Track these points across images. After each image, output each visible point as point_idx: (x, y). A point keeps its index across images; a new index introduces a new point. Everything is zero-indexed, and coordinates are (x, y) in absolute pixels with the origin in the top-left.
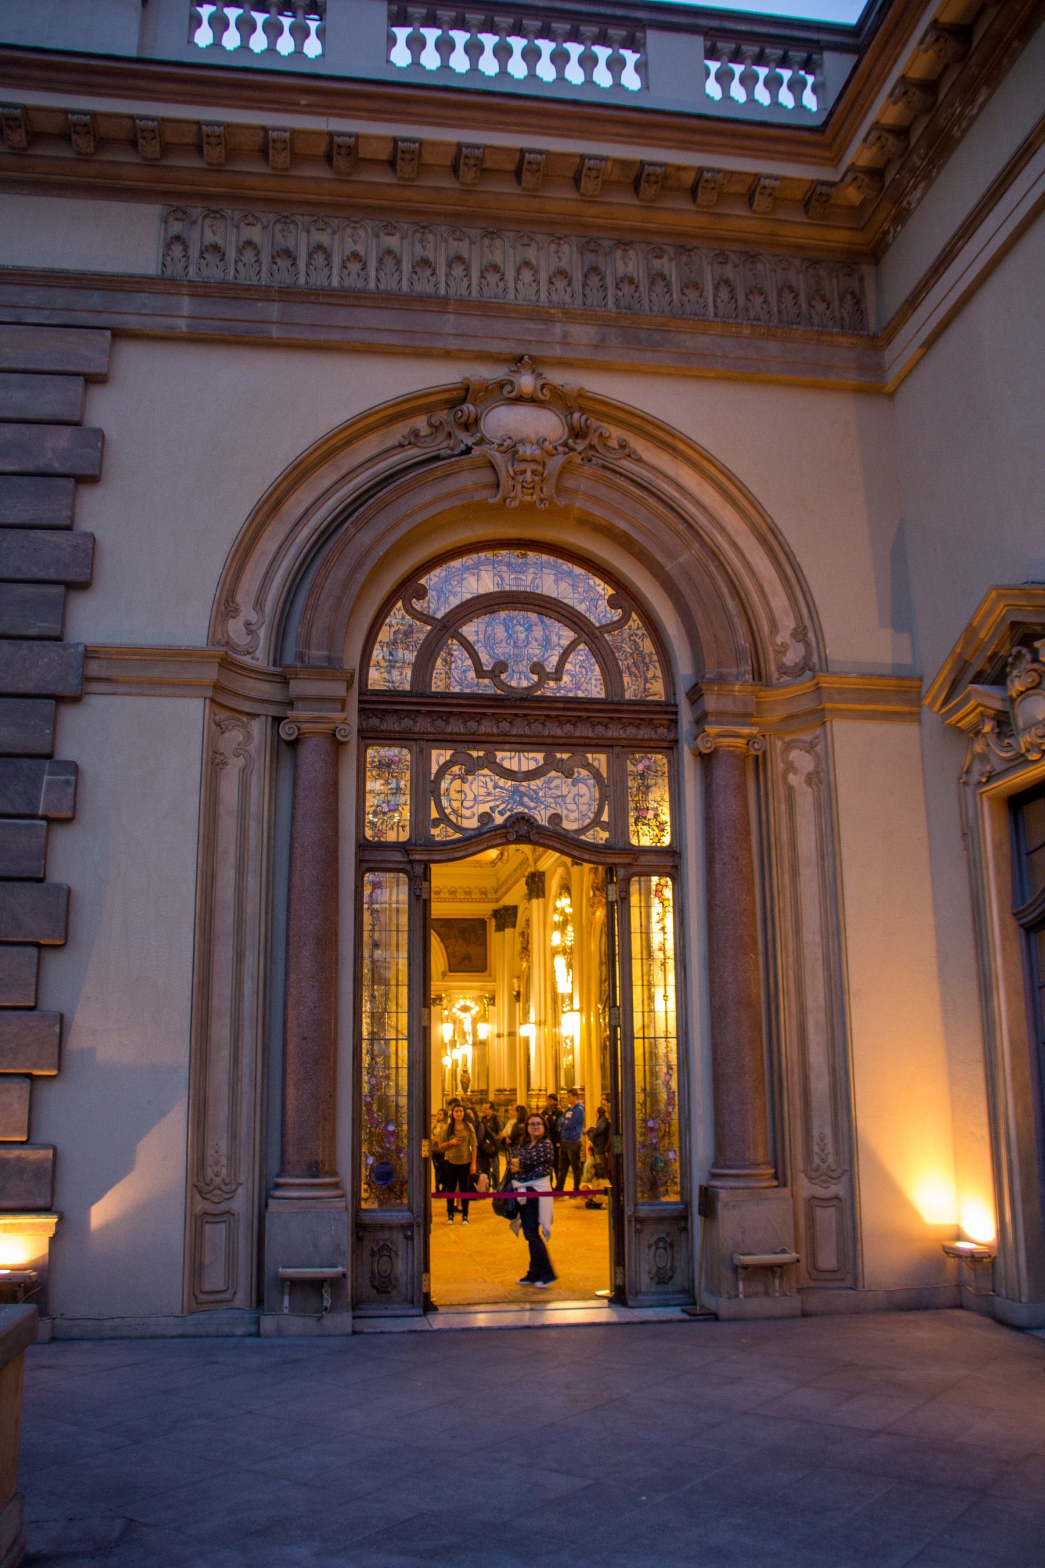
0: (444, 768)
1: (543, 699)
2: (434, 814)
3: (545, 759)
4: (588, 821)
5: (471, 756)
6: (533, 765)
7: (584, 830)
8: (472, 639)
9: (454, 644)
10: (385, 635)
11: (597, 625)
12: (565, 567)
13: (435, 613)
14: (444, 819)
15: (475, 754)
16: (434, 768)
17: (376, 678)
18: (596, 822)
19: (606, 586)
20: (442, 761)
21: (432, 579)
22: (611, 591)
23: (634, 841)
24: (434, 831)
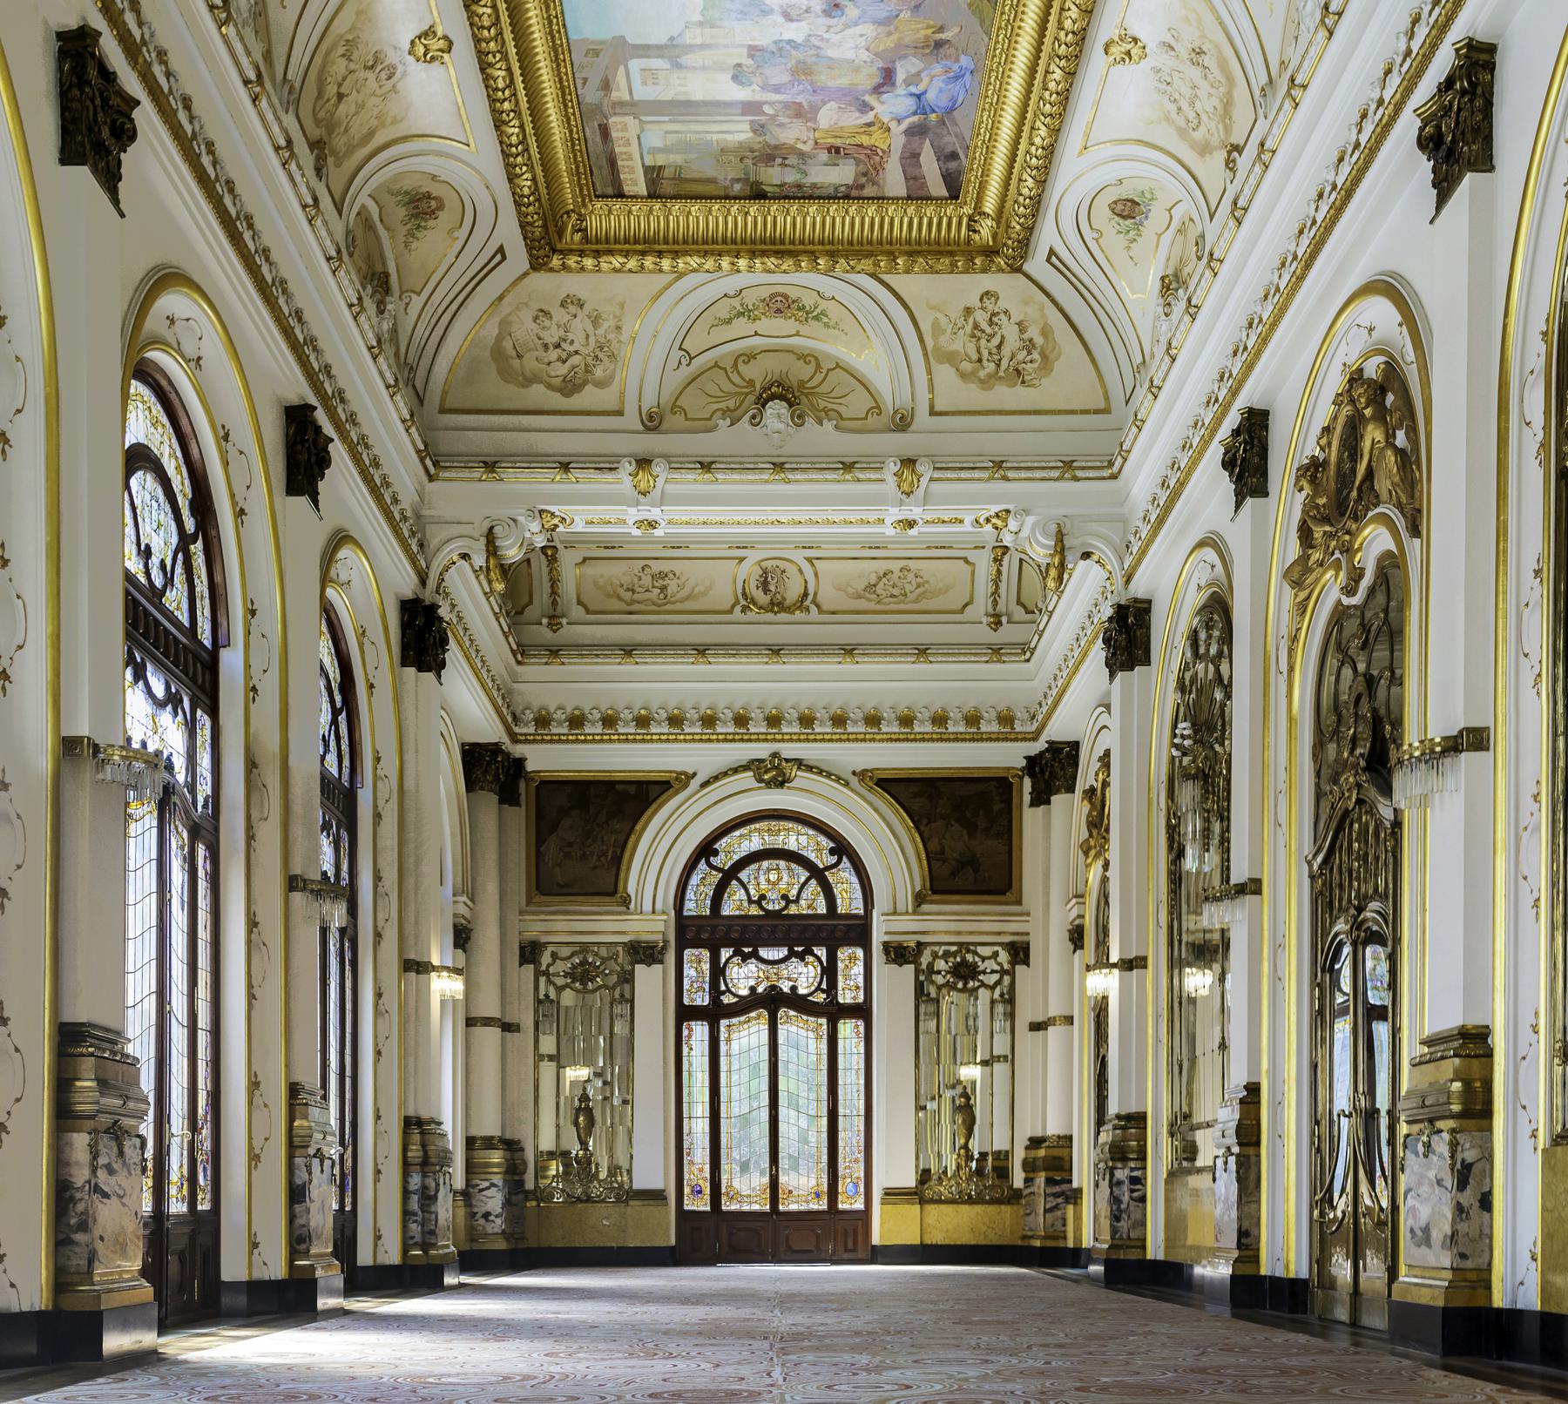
1: (788, 916)
7: (811, 994)
8: (745, 880)
10: (695, 879)
14: (728, 990)
15: (746, 950)
16: (723, 960)
17: (690, 908)
18: (818, 988)
21: (722, 844)
22: (832, 845)
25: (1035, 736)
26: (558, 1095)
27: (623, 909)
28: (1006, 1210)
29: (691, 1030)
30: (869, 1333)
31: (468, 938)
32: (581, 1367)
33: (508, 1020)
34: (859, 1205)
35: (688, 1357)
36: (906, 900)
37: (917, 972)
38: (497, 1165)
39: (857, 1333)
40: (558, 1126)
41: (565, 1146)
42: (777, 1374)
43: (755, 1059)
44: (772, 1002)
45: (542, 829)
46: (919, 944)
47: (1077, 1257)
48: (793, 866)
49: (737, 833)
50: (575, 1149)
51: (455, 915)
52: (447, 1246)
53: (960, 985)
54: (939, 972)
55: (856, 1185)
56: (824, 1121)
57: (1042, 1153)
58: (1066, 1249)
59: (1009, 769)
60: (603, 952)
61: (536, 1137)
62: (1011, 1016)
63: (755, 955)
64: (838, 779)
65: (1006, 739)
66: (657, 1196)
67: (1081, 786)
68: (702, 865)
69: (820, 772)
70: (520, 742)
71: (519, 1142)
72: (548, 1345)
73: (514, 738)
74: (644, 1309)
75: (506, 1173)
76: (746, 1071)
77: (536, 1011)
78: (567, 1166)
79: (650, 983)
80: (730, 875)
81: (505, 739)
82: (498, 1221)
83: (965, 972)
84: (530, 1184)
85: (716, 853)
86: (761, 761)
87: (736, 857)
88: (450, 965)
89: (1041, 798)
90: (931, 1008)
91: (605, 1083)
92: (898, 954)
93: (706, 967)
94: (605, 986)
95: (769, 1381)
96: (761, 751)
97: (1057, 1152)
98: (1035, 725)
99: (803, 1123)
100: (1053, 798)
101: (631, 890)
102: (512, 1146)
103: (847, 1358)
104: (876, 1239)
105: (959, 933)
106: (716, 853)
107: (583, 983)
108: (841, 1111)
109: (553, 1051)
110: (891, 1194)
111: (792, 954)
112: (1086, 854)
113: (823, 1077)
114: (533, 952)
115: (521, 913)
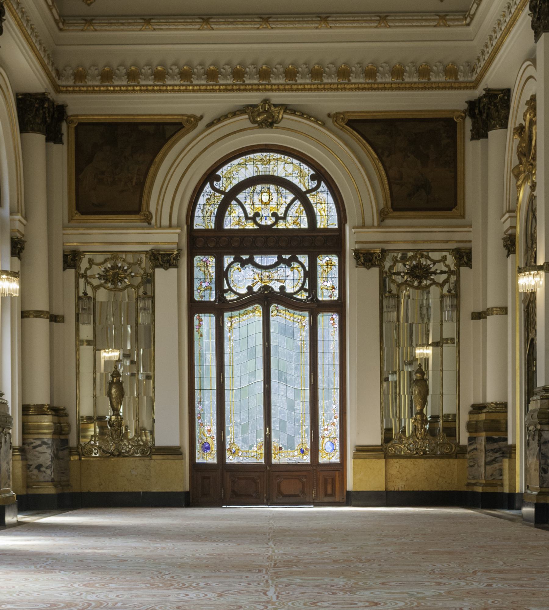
0: (229, 266)
2: (226, 287)
3: (278, 258)
4: (297, 288)
5: (242, 258)
6: (273, 263)
7: (296, 293)
8: (243, 201)
9: (234, 202)
10: (202, 200)
11: (304, 190)
12: (289, 160)
13: (225, 189)
14: (230, 289)
15: (244, 257)
16: (226, 265)
17: (198, 224)
18: (302, 288)
19: (310, 169)
20: (229, 262)
22: (312, 172)
23: (320, 299)
24: (225, 295)
25: (475, 85)
26: (95, 372)
27: (146, 224)
28: (454, 463)
29: (200, 320)
30: (345, 561)
31: (22, 249)
32: (112, 596)
33: (55, 312)
34: (335, 459)
35: (197, 588)
36: (372, 216)
37: (381, 273)
38: (47, 427)
39: (335, 561)
40: (95, 396)
41: (101, 413)
42: (271, 593)
43: (251, 344)
44: (266, 298)
45: (82, 160)
46: (383, 251)
47: (510, 501)
48: (281, 189)
49: (235, 162)
50: (109, 415)
51: (12, 231)
52: (8, 492)
53: (416, 284)
54: (398, 274)
55: (333, 444)
56: (307, 393)
57: (483, 417)
58: (502, 494)
59: (453, 111)
60: (130, 259)
61: (77, 405)
62: (457, 307)
63: (251, 261)
64: (316, 120)
65: (451, 88)
66: (173, 452)
67: (513, 122)
68: (208, 188)
69: (302, 115)
70: (62, 92)
71: (64, 409)
72: (86, 577)
73: (58, 89)
74: (163, 545)
75: (54, 433)
76: (245, 353)
77: (77, 306)
78: (102, 428)
79: (167, 282)
80: (230, 196)
81: (51, 90)
82: (49, 472)
83: (420, 273)
84: (73, 443)
85: (218, 179)
86: (255, 106)
87: (235, 182)
88: (8, 269)
89: (480, 133)
90: (393, 302)
91: (132, 362)
92: (366, 259)
93: (212, 270)
94: (131, 286)
95: (265, 599)
96: (254, 98)
97: (494, 416)
98: (475, 77)
99: (291, 395)
100: (490, 133)
101: (152, 208)
102: (58, 412)
103: (327, 580)
104: (350, 486)
105: (415, 242)
106: (218, 179)
107: (114, 283)
108: (320, 385)
109: (91, 338)
110: (362, 451)
111: (281, 261)
112: (517, 177)
113: (306, 358)
114: (74, 259)
115: (64, 227)
